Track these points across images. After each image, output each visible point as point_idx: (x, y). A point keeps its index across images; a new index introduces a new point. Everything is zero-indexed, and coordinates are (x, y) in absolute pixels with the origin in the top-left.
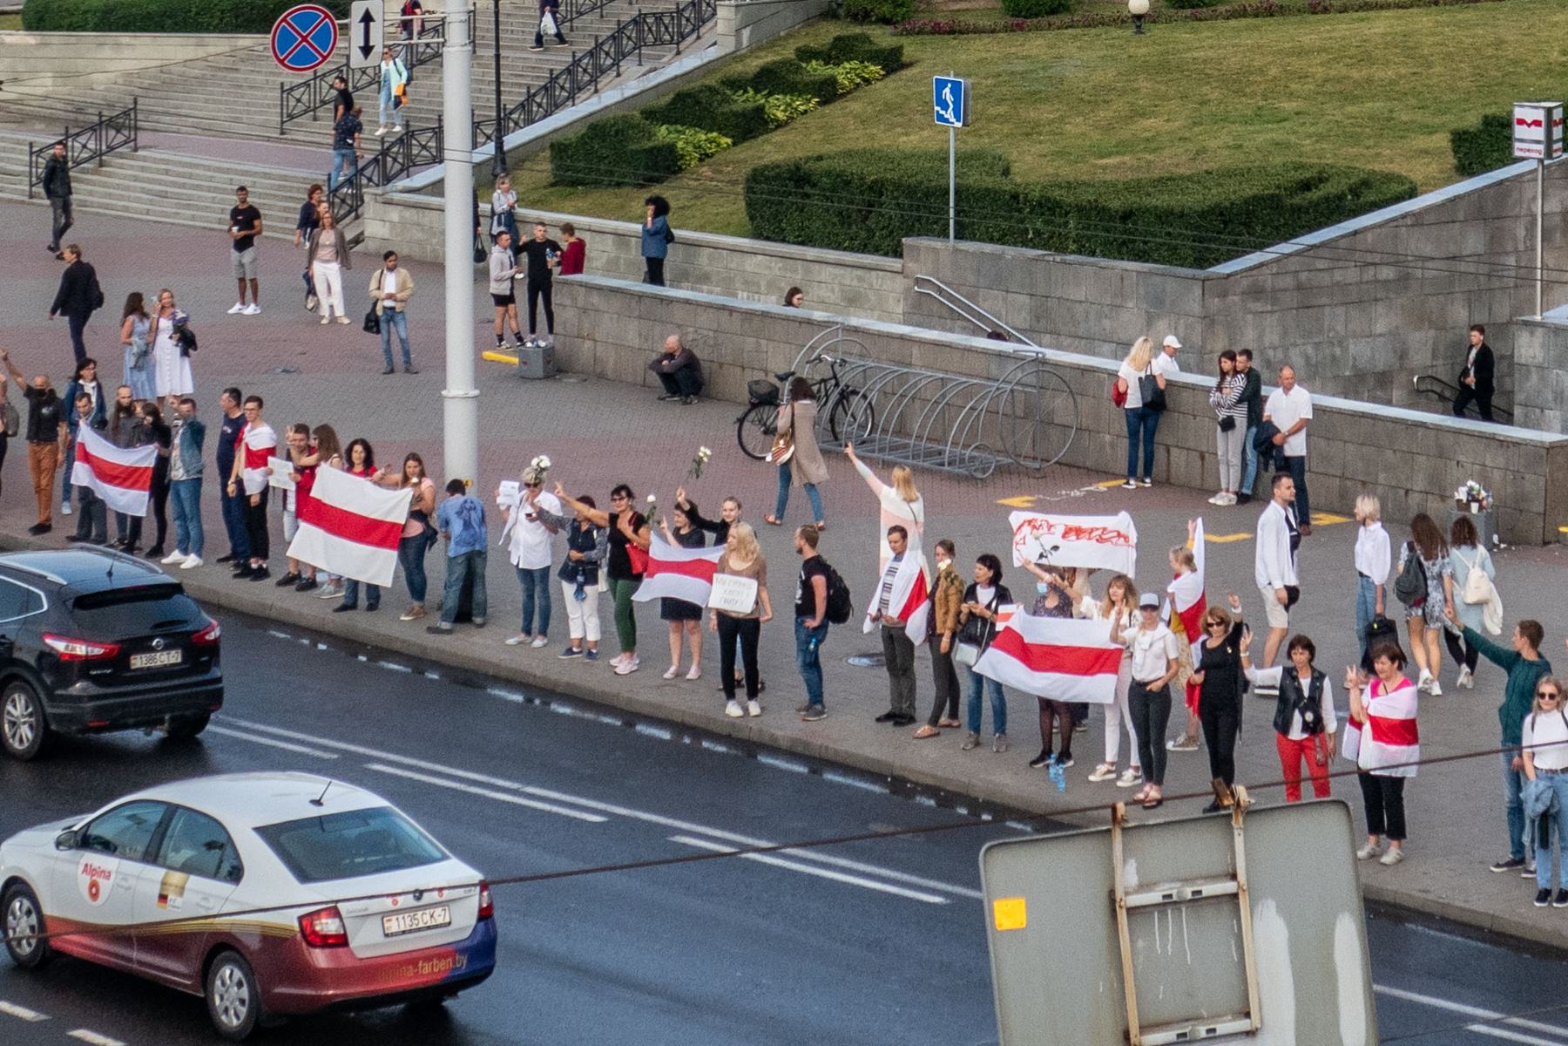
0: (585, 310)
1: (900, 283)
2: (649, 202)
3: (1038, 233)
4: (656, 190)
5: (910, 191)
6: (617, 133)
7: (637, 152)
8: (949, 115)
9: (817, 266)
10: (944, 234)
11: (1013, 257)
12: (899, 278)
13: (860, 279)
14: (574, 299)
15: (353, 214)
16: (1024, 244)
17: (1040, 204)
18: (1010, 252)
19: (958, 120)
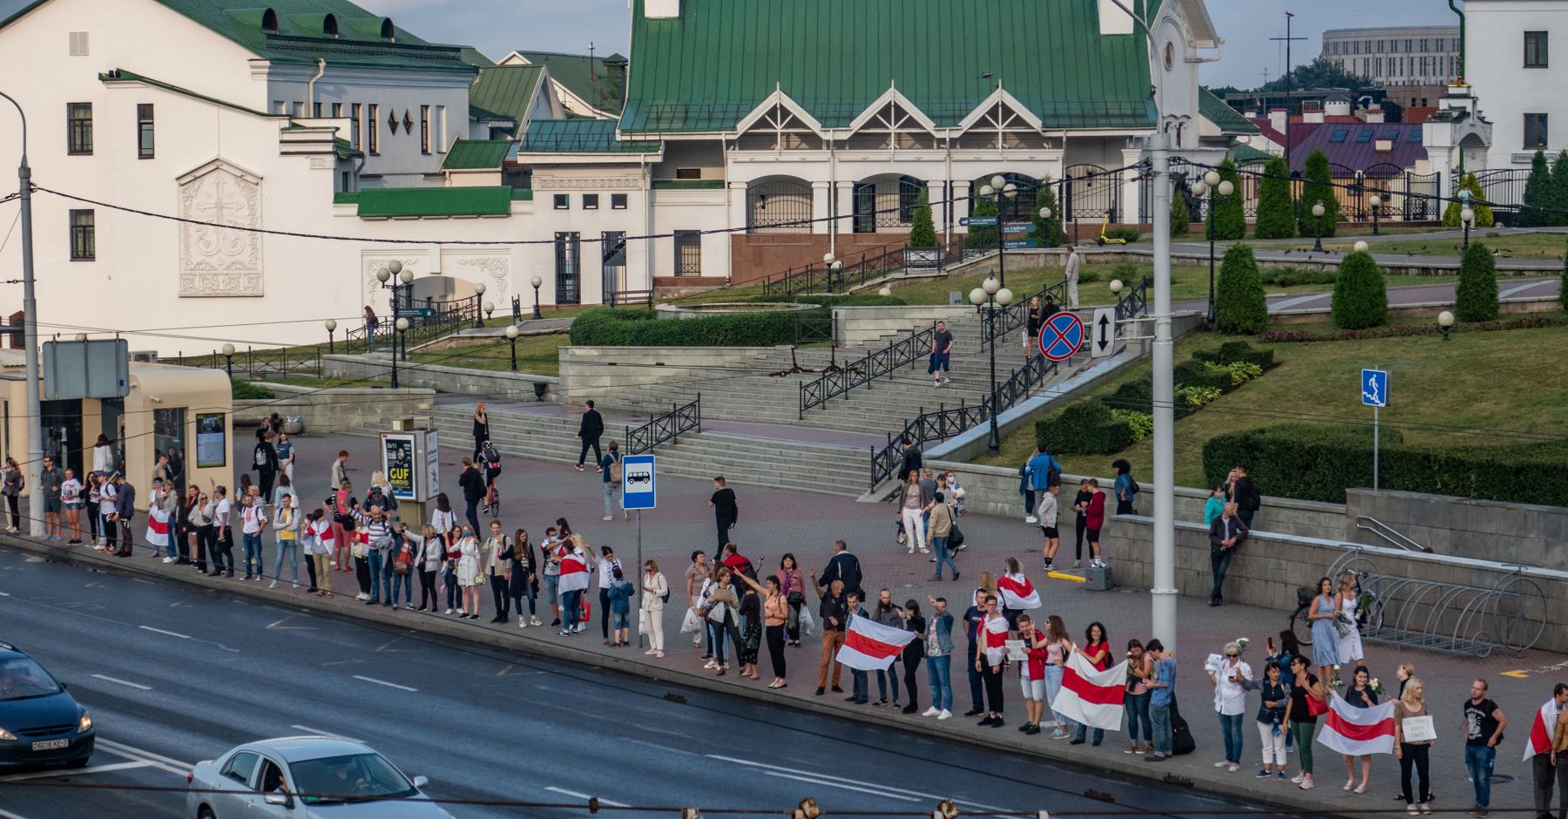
0: (1134, 541)
1: (1344, 521)
2: (1115, 465)
3: (1445, 484)
4: (1118, 457)
5: (1341, 454)
6: (1088, 413)
7: (1103, 429)
8: (1375, 398)
9: (1275, 510)
10: (1369, 485)
11: (1437, 502)
12: (1343, 518)
13: (1311, 519)
14: (1125, 534)
15: (887, 477)
16: (1434, 492)
17: (1447, 463)
18: (1435, 498)
19: (1382, 402)
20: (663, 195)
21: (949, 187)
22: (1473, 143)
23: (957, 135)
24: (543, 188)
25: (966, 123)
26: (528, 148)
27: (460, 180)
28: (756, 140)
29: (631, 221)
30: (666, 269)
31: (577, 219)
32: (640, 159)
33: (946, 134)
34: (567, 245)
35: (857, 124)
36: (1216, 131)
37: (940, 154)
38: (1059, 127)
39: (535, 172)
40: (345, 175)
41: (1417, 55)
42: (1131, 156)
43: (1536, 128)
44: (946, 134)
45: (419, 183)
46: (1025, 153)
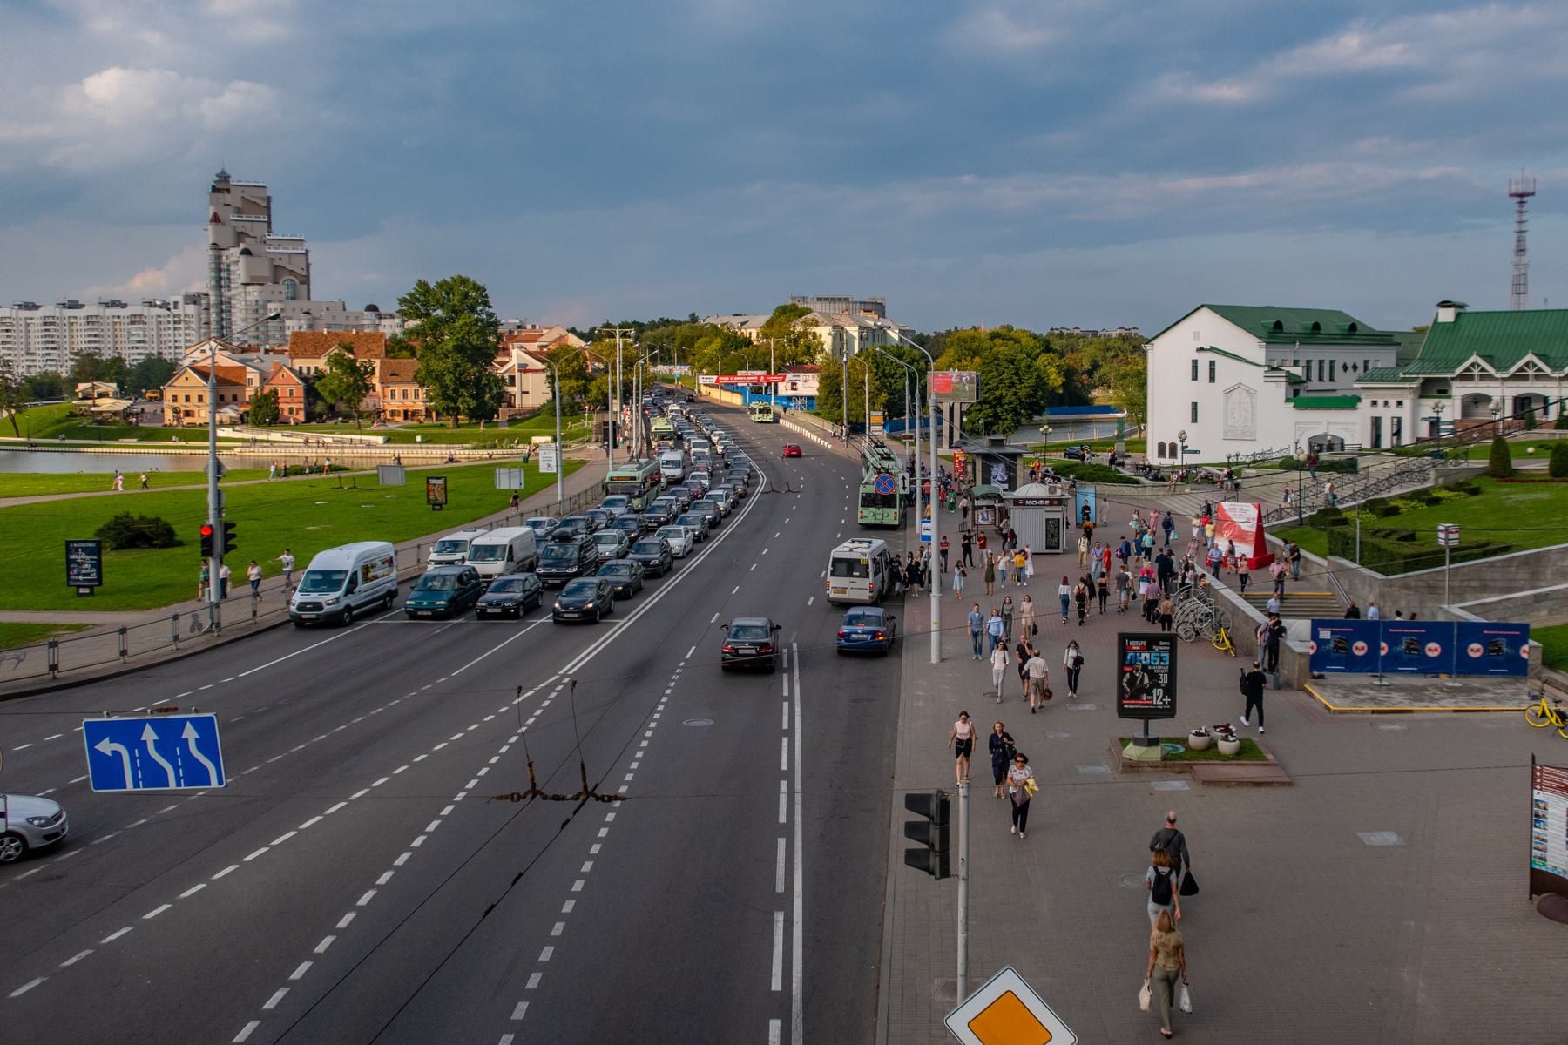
23: (1562, 375)
24: (1367, 396)
28: (1466, 377)
29: (1405, 413)
31: (1380, 411)
32: (1407, 385)
33: (1556, 375)
34: (1376, 422)
35: (1513, 370)
40: (1296, 393)
44: (1556, 375)
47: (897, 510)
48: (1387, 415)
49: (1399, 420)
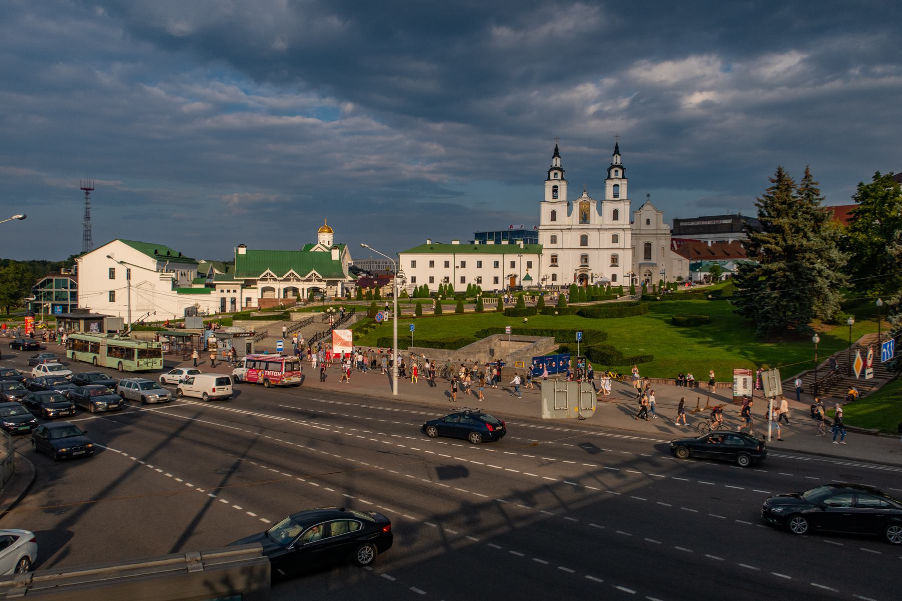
20: (244, 290)
21: (303, 290)
22: (404, 282)
24: (219, 288)
25: (307, 277)
26: (215, 280)
27: (195, 286)
29: (237, 295)
30: (244, 305)
31: (225, 295)
33: (303, 279)
34: (223, 300)
35: (284, 277)
36: (352, 279)
37: (302, 283)
38: (325, 278)
39: (217, 285)
41: (385, 265)
42: (340, 284)
43: (414, 280)
44: (303, 279)
45: (187, 287)
46: (318, 283)
47: (162, 359)
48: (229, 297)
49: (235, 299)
